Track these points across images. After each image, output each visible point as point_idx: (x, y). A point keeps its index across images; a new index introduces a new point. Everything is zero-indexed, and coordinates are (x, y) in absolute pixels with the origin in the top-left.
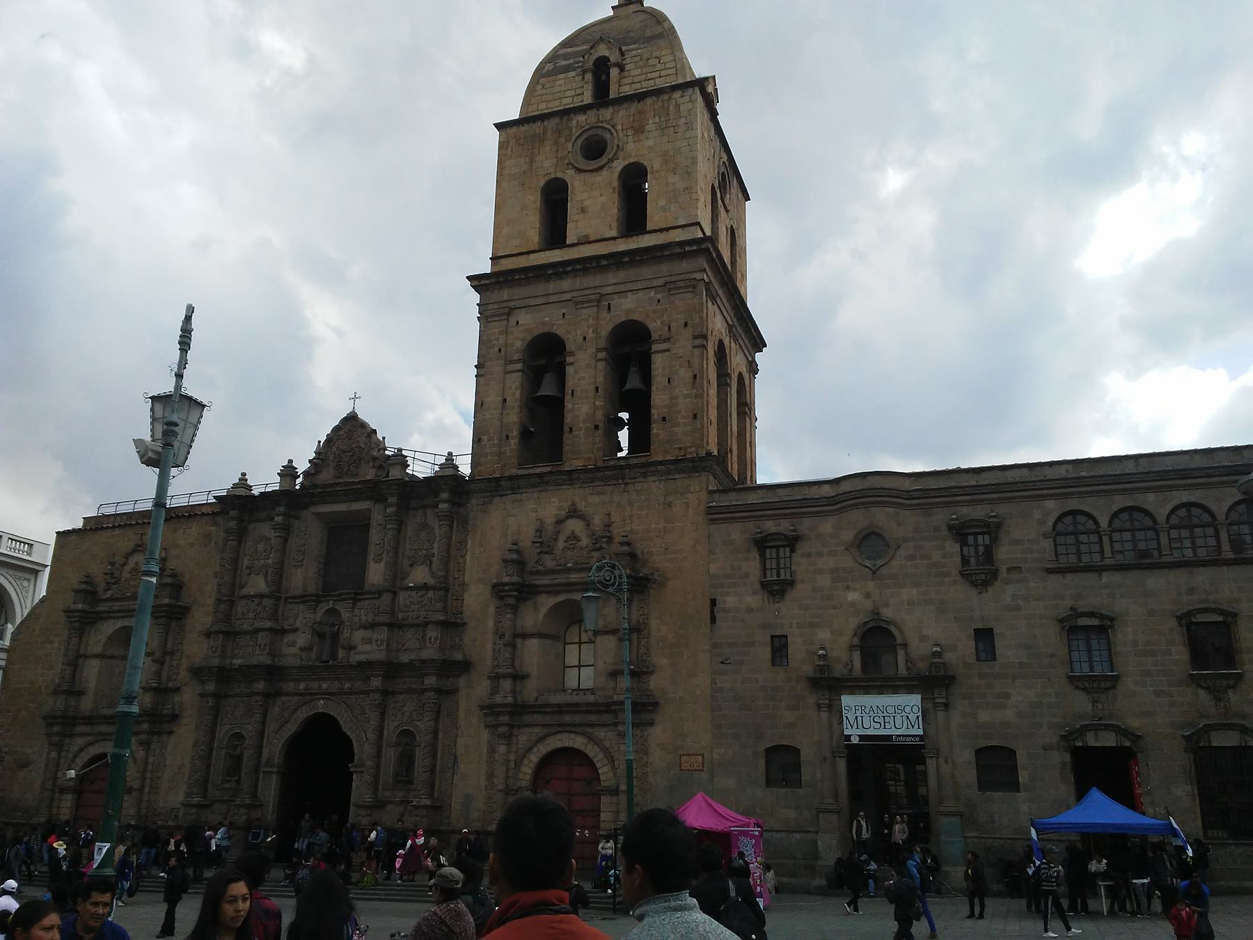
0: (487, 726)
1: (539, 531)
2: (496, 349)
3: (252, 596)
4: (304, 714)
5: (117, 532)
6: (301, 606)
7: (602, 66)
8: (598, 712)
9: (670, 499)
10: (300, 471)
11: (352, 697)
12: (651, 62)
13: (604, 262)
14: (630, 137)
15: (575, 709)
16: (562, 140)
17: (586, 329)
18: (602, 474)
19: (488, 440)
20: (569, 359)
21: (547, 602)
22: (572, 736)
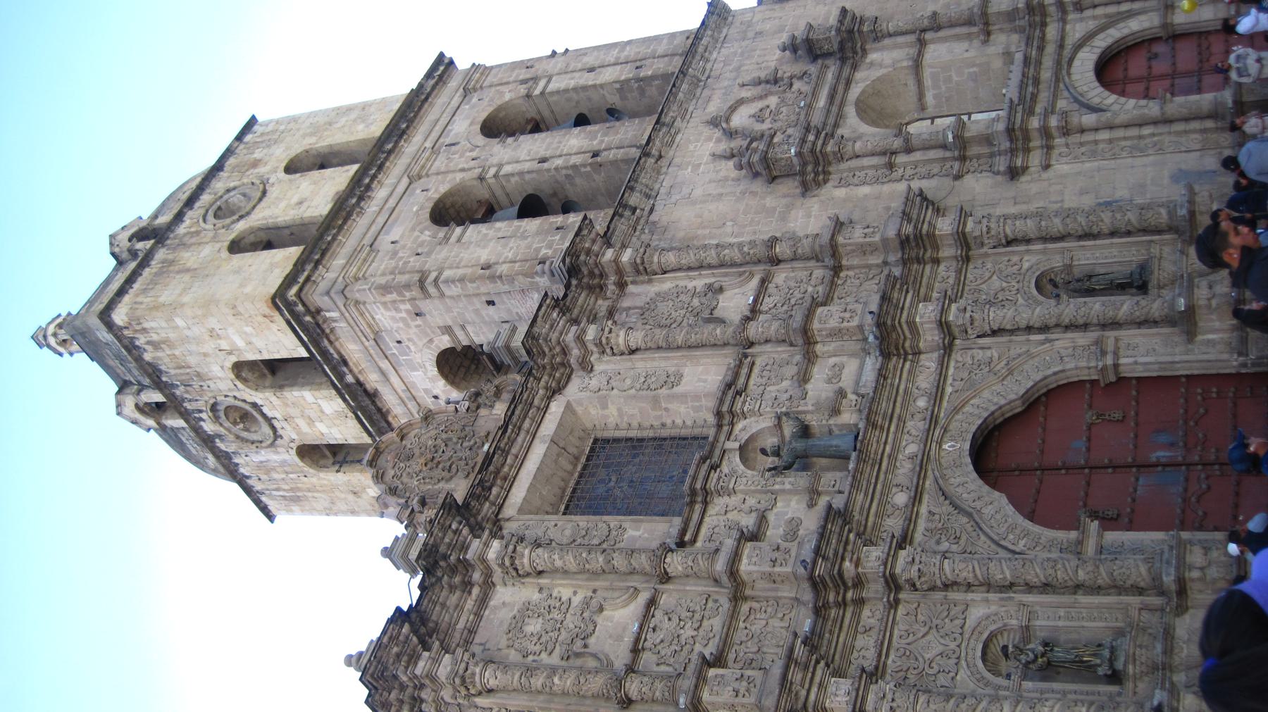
0: (1047, 167)
3: (641, 627)
4: (966, 482)
6: (712, 510)
8: (1043, 38)
9: (751, 34)
11: (949, 389)
13: (389, 146)
14: (256, 171)
15: (1033, 61)
18: (680, 94)
19: (549, 246)
21: (853, 124)
22: (1076, 63)
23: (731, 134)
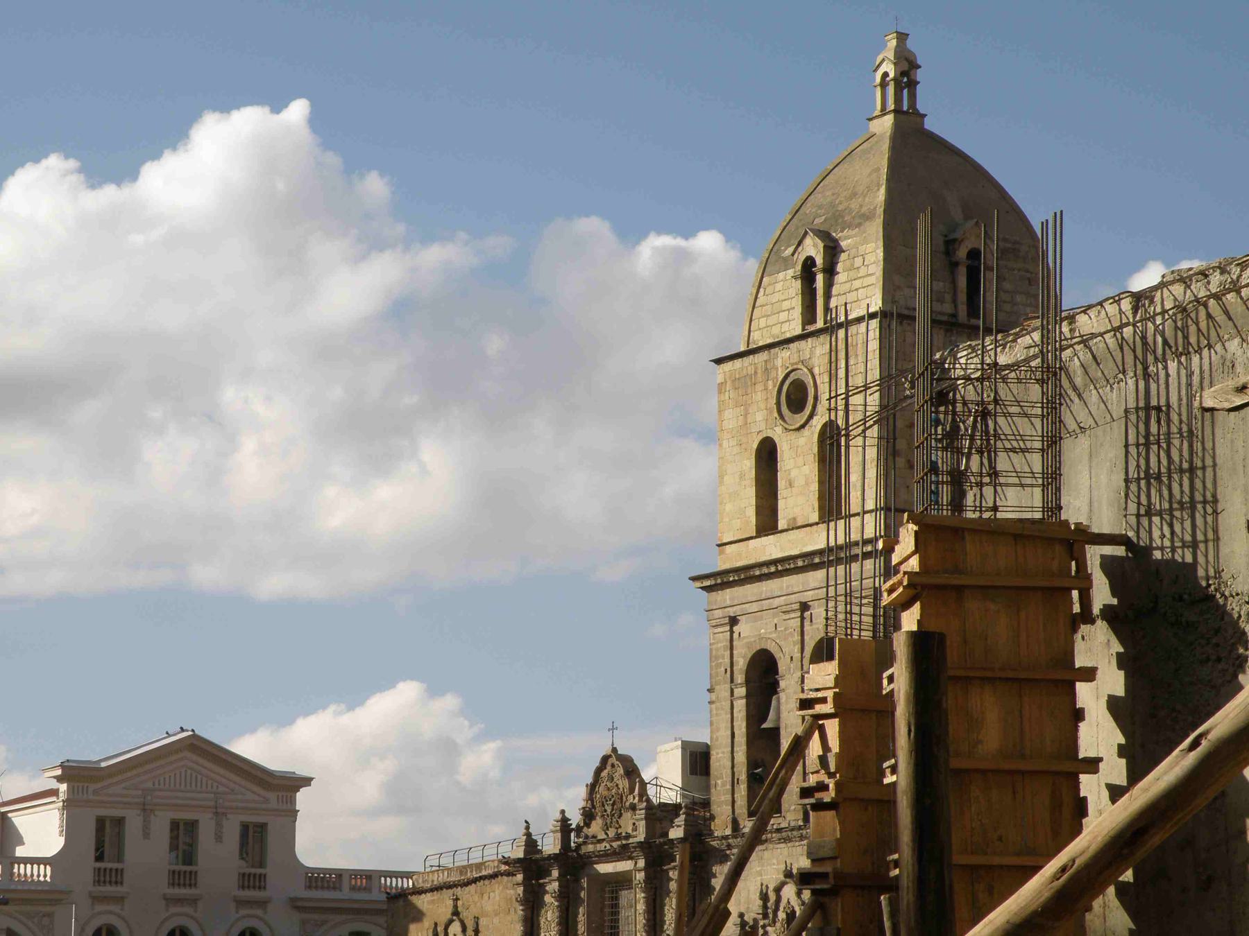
1: (764, 897)
2: (723, 669)
5: (436, 895)
7: (809, 263)
10: (573, 826)
12: (858, 262)
16: (770, 383)
17: (792, 647)
19: (724, 785)
20: (782, 684)
23: (778, 890)
